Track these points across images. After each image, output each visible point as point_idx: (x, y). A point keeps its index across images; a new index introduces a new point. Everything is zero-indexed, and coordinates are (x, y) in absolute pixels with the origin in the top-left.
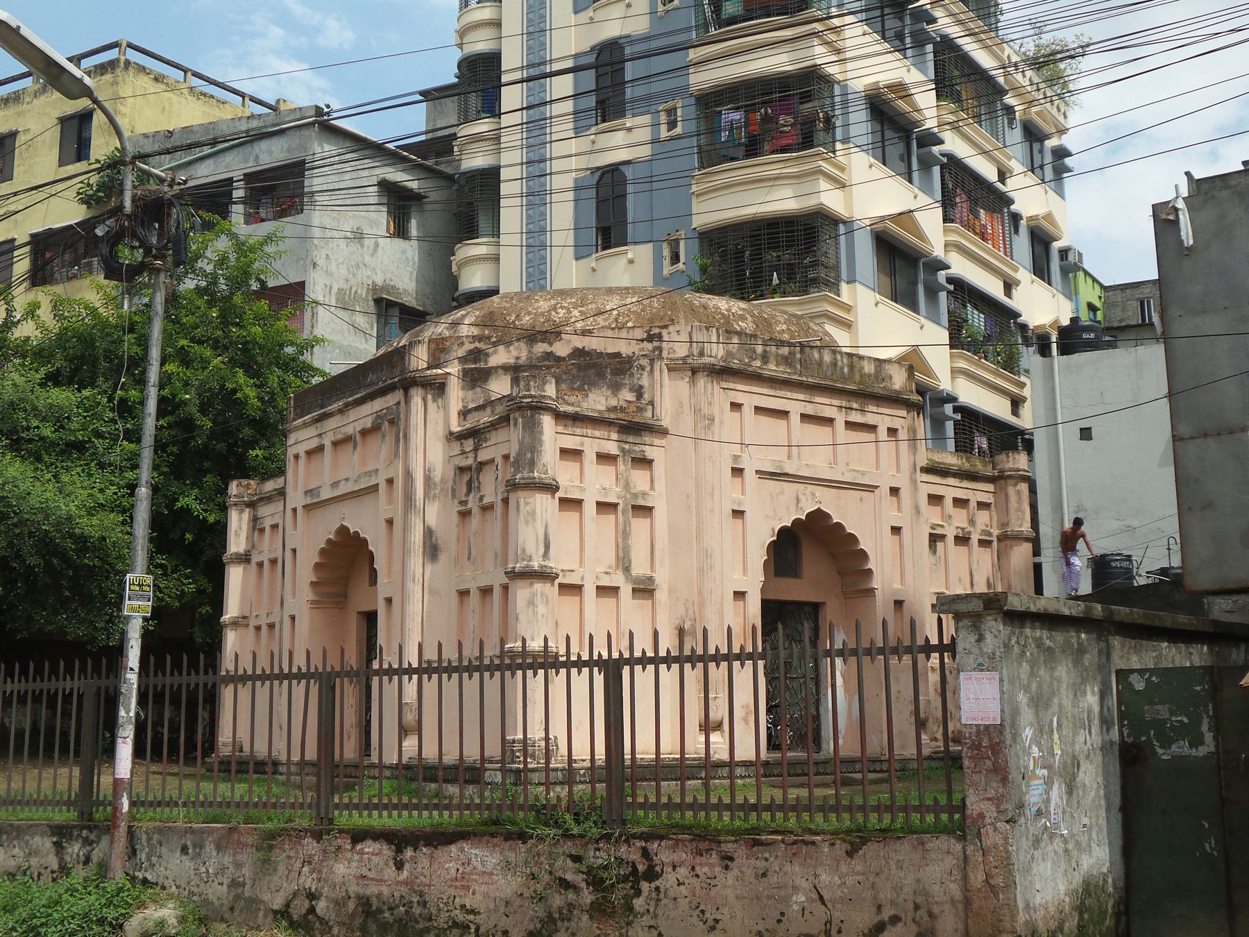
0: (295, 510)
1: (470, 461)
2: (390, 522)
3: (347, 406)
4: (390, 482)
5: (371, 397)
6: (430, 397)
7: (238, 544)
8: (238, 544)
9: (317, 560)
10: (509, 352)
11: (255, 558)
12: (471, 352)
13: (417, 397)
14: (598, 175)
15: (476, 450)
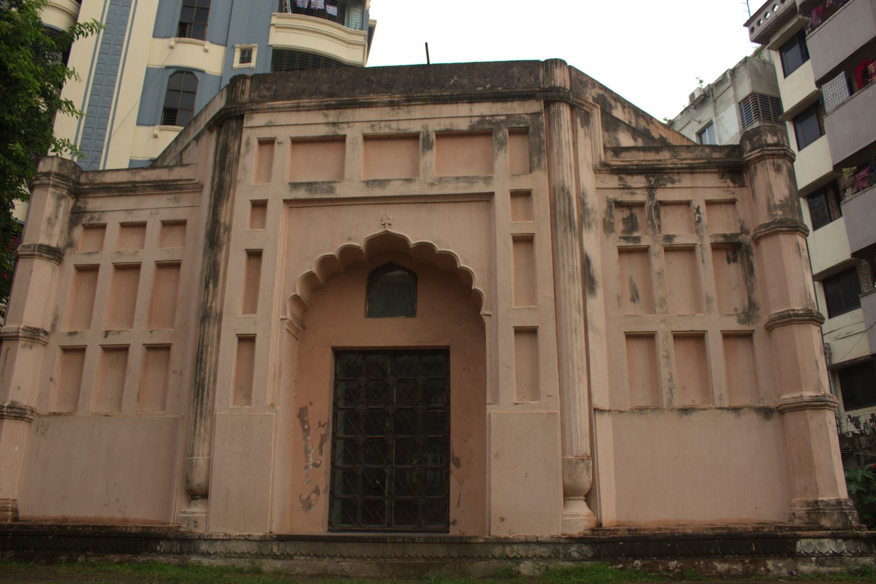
0: (260, 205)
1: (640, 197)
2: (524, 241)
3: (410, 101)
4: (521, 195)
5: (472, 99)
6: (578, 120)
7: (50, 236)
8: (50, 236)
9: (314, 269)
10: (624, 113)
11: (72, 260)
12: (599, 95)
13: (565, 112)
14: (172, 71)
15: (651, 189)
